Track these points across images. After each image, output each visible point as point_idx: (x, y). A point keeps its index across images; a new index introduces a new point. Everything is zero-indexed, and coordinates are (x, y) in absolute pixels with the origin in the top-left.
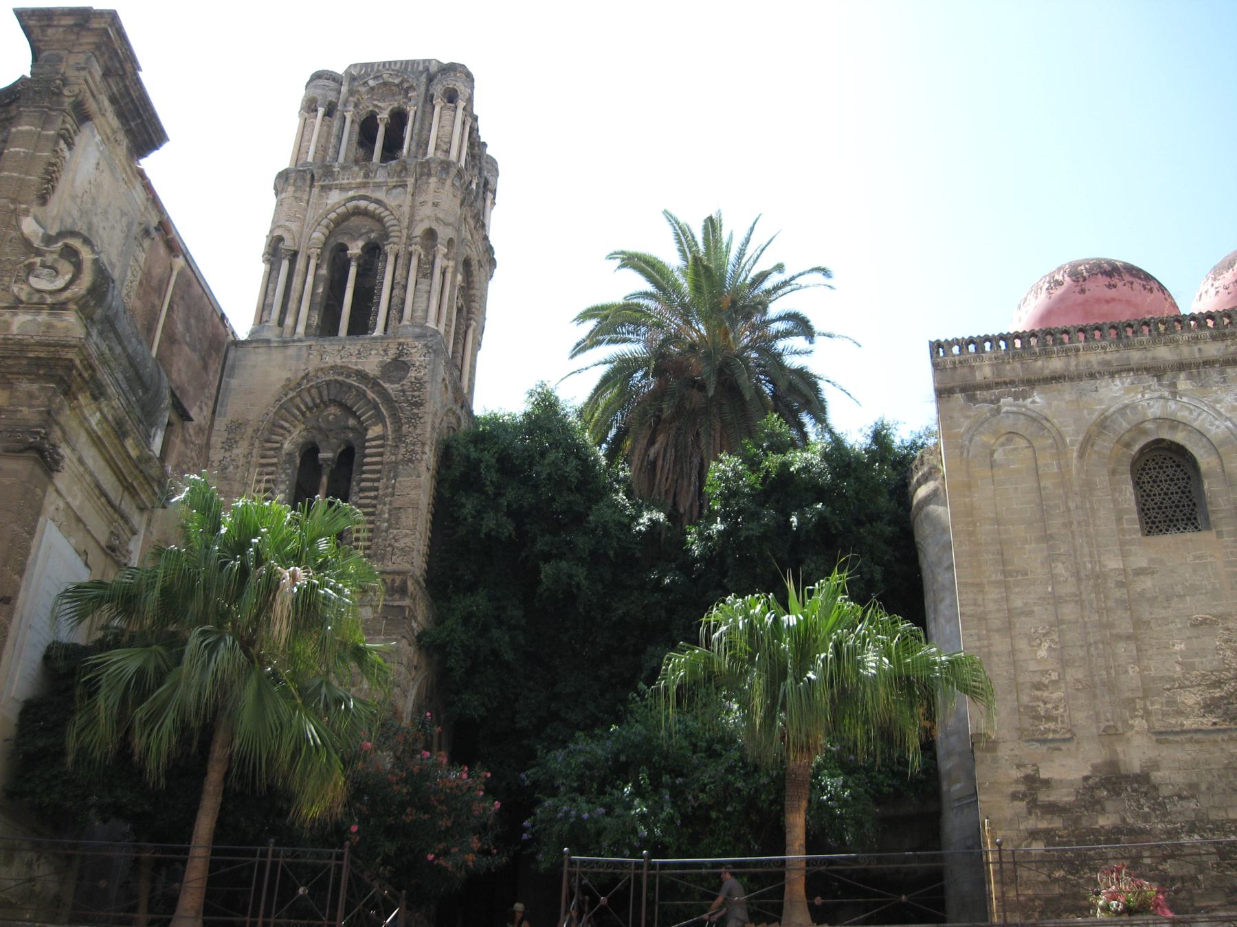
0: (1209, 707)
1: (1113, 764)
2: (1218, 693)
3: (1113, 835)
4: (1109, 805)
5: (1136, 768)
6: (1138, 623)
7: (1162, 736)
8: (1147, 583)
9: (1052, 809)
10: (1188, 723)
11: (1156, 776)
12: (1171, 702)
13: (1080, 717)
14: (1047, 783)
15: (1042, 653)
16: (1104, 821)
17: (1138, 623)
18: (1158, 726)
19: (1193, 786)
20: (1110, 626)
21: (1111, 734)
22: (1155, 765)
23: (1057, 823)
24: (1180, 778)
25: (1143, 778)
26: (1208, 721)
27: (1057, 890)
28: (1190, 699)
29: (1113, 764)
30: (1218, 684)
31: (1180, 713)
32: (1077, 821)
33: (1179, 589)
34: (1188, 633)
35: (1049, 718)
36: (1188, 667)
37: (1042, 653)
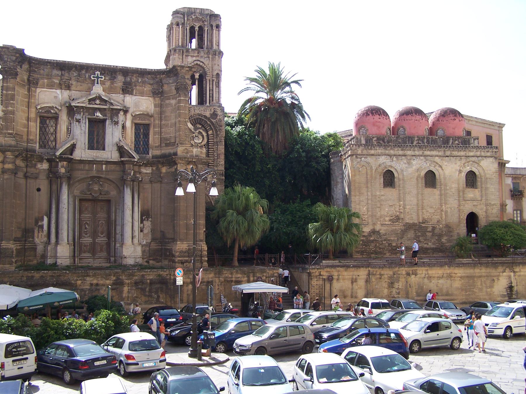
0: (390, 220)
1: (374, 229)
2: (392, 218)
3: (373, 241)
4: (373, 236)
5: (378, 230)
6: (381, 205)
7: (382, 225)
8: (383, 198)
9: (364, 236)
10: (387, 223)
11: (381, 231)
12: (384, 219)
13: (370, 221)
14: (364, 232)
15: (365, 209)
16: (372, 239)
17: (381, 205)
18: (382, 223)
19: (386, 233)
20: (376, 205)
21: (374, 224)
22: (381, 230)
23: (364, 239)
24: (384, 232)
25: (378, 232)
26: (389, 223)
27: (363, 249)
28: (387, 219)
29: (374, 229)
30: (392, 217)
31: (385, 221)
32: (367, 238)
33: (388, 199)
34: (389, 207)
35: (365, 221)
36: (388, 213)
37: (365, 209)
